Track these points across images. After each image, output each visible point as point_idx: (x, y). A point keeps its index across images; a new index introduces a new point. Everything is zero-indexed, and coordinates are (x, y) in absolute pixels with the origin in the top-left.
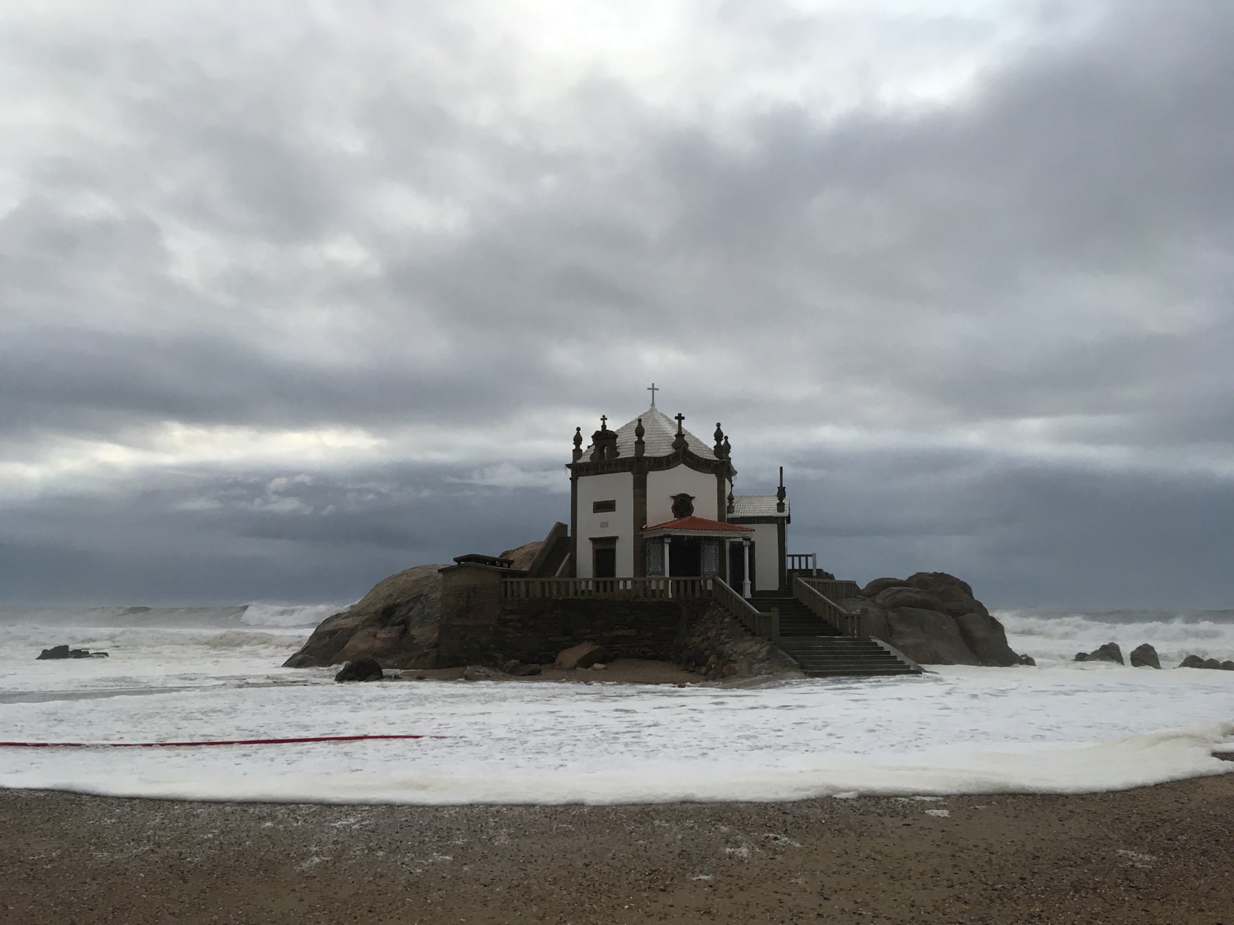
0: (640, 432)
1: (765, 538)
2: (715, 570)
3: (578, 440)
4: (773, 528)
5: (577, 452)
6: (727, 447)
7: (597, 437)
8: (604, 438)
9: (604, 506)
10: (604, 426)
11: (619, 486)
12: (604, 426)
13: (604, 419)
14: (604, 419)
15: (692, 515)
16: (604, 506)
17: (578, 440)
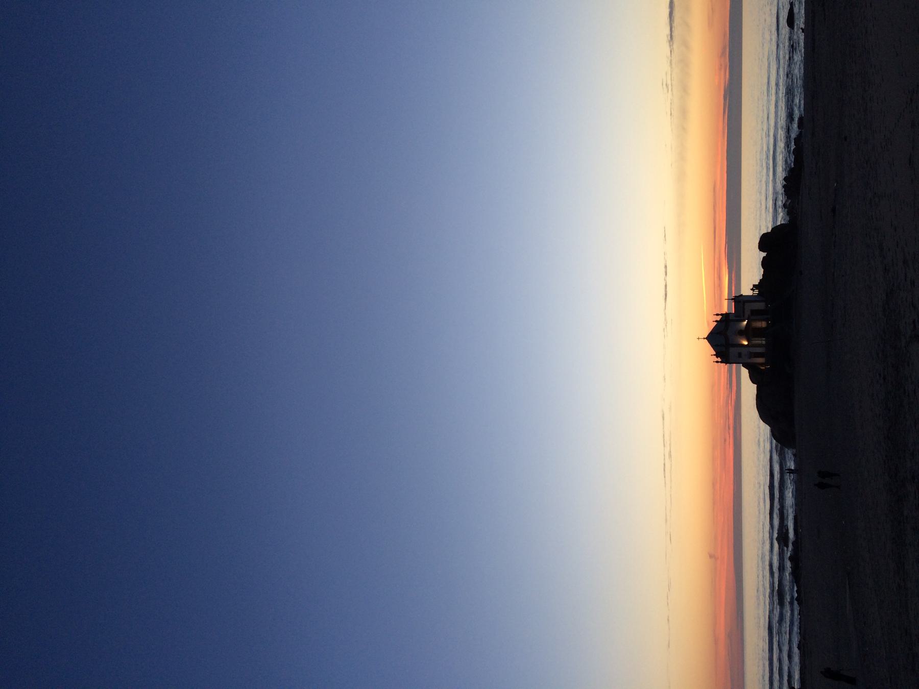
0: (717, 346)
1: (749, 307)
2: (760, 323)
3: (717, 362)
4: (746, 304)
5: (721, 362)
6: (717, 315)
7: (717, 357)
8: (717, 355)
9: (740, 355)
10: (714, 355)
11: (733, 351)
12: (714, 355)
13: (712, 355)
14: (712, 355)
15: (743, 329)
16: (740, 355)
17: (717, 362)
